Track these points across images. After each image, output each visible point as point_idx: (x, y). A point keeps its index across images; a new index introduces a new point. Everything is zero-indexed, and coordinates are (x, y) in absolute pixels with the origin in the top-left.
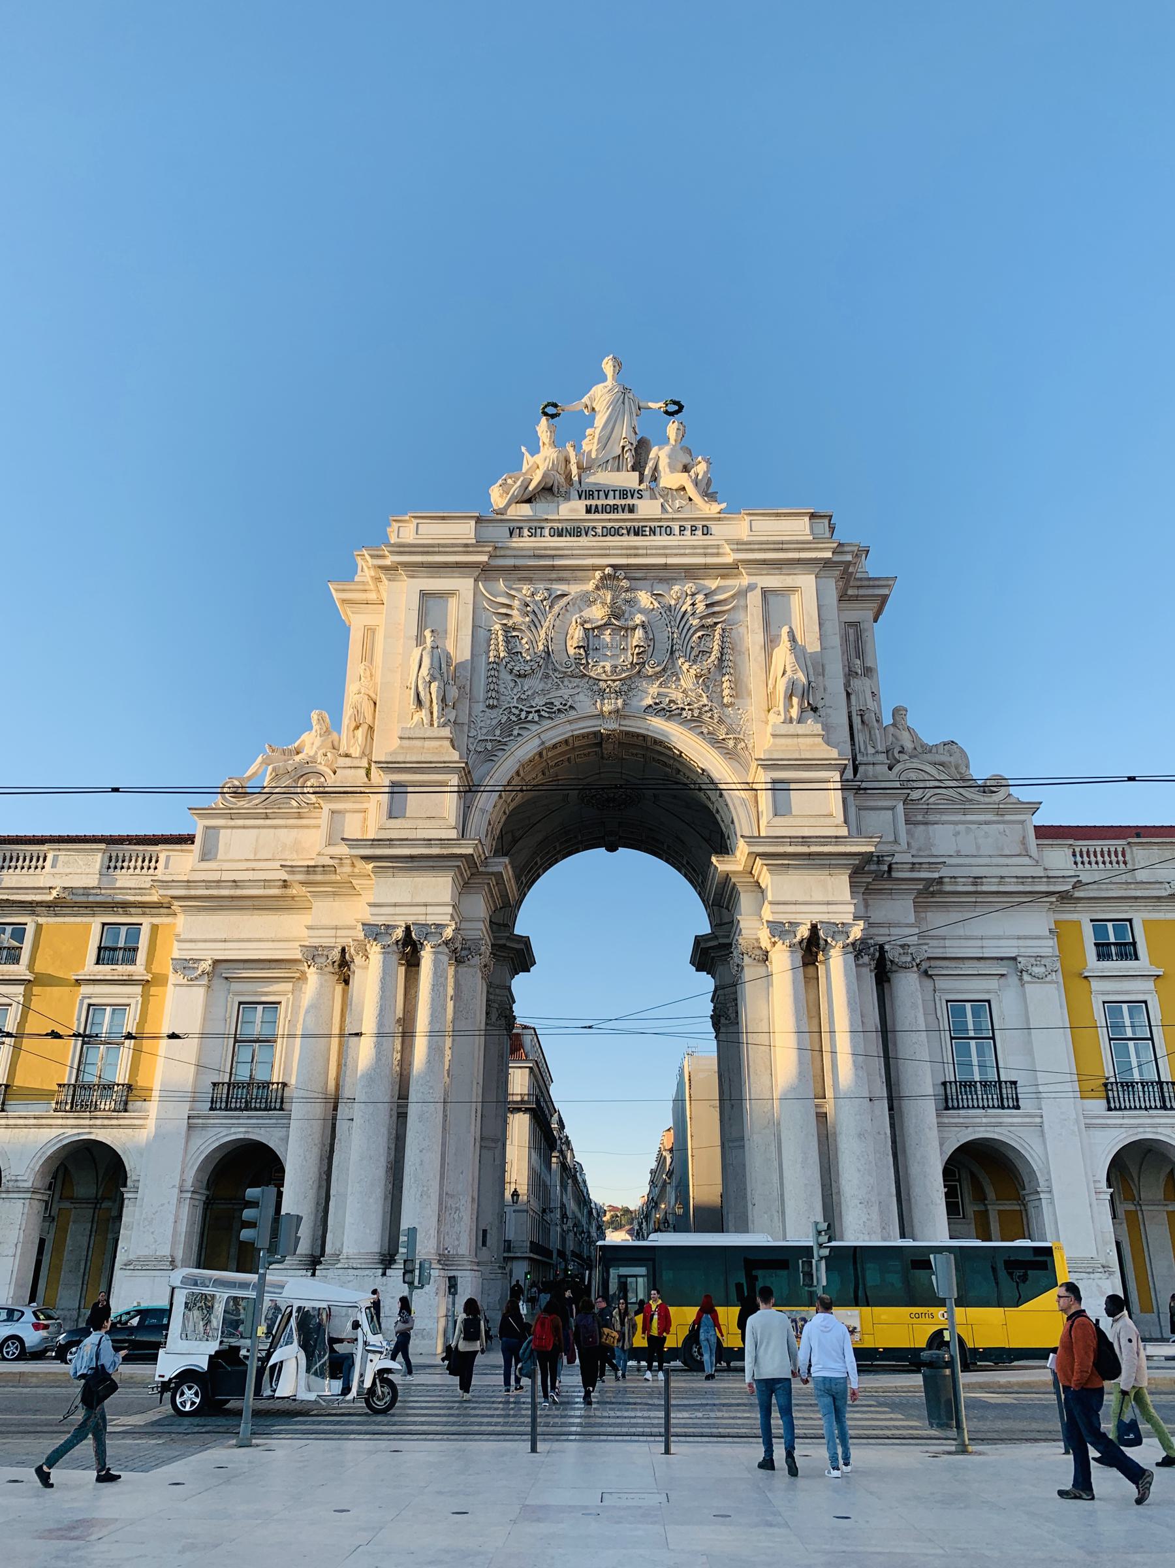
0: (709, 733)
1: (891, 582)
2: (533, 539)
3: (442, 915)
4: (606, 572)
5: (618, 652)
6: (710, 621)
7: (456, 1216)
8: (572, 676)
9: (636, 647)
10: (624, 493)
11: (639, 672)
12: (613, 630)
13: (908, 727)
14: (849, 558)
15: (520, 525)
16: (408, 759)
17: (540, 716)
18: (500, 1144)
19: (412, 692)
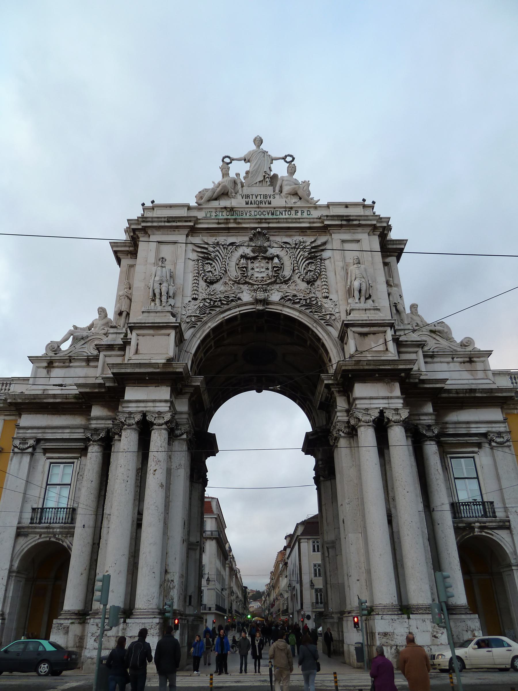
0: (315, 312)
1: (405, 242)
3: (164, 407)
4: (257, 231)
5: (263, 270)
6: (313, 255)
7: (171, 587)
8: (239, 283)
9: (275, 267)
10: (265, 196)
11: (276, 280)
12: (261, 259)
13: (419, 316)
14: (385, 225)
18: (199, 548)
19: (151, 290)
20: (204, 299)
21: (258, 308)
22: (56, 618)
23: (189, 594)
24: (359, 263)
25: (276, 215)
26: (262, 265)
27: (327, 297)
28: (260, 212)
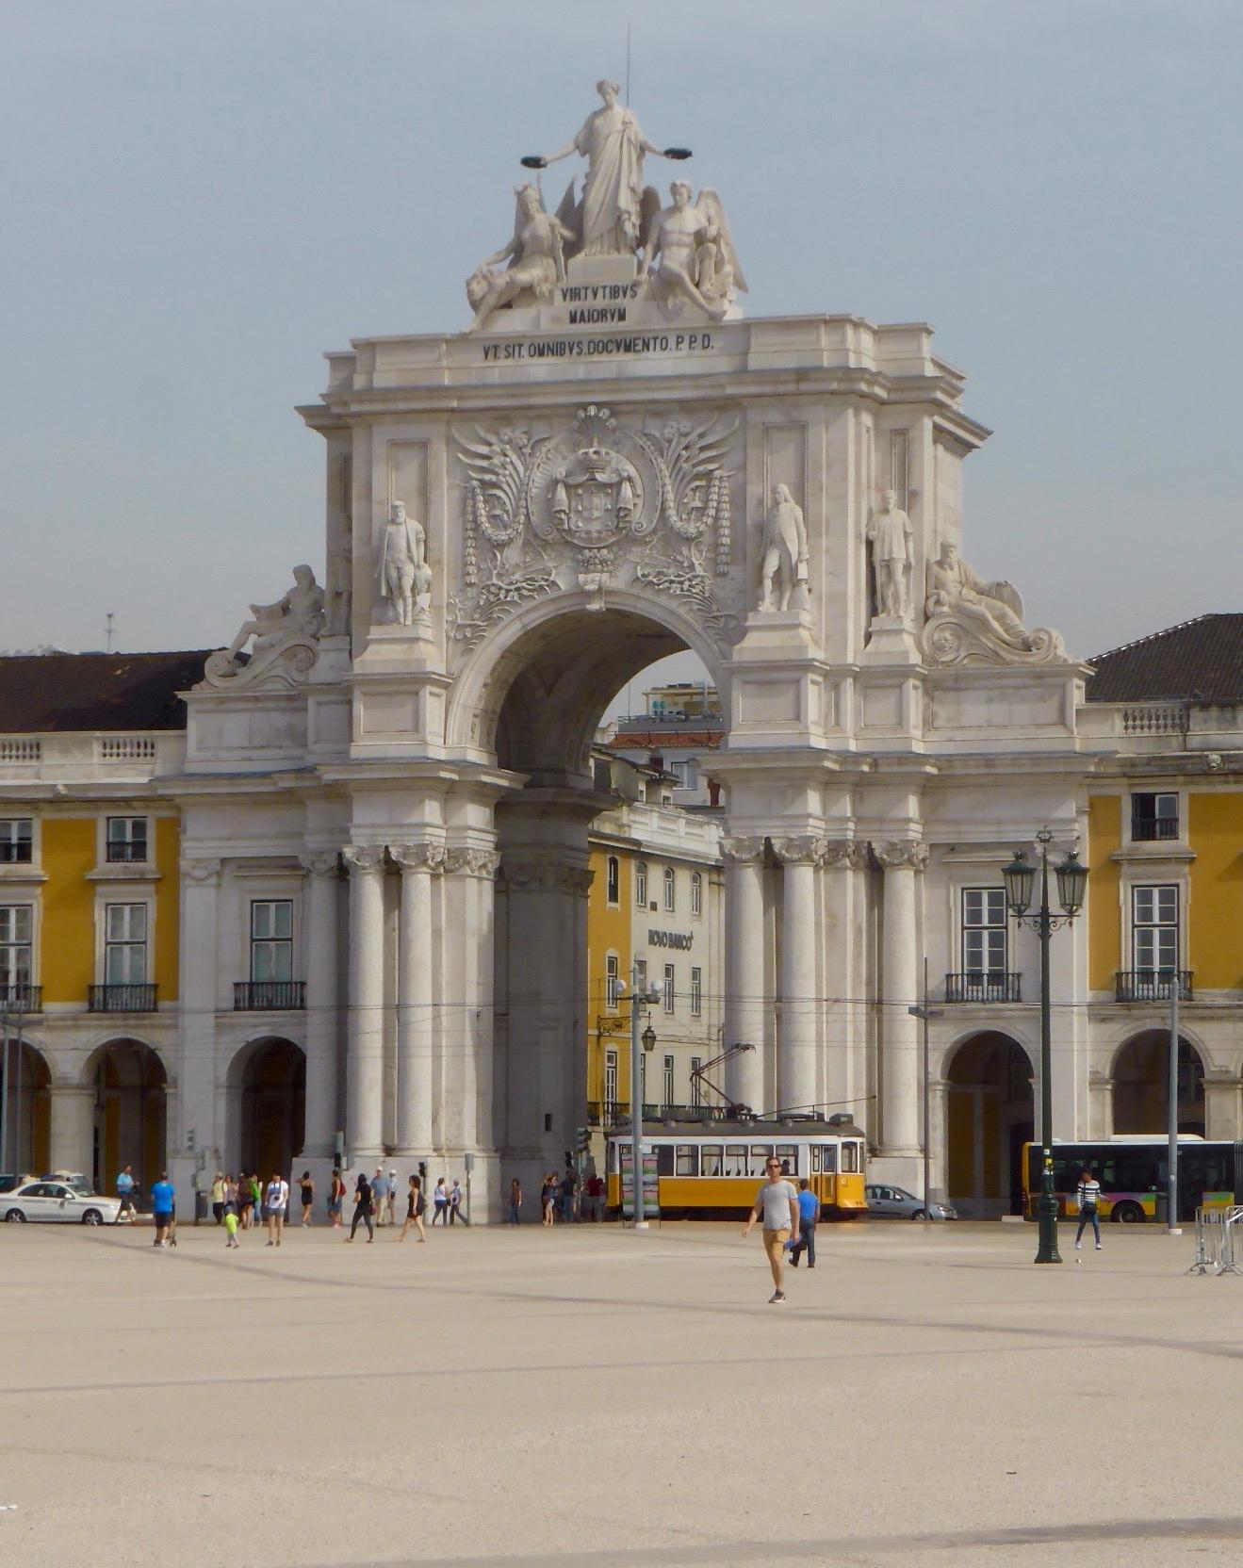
2: (510, 362)
6: (700, 468)
9: (620, 508)
10: (615, 292)
11: (627, 535)
15: (495, 343)
16: (377, 671)
17: (521, 597)
20: (488, 585)
21: (588, 607)
22: (296, 1156)
23: (545, 1110)
24: (786, 501)
25: (635, 351)
26: (596, 501)
27: (723, 575)
28: (601, 344)
